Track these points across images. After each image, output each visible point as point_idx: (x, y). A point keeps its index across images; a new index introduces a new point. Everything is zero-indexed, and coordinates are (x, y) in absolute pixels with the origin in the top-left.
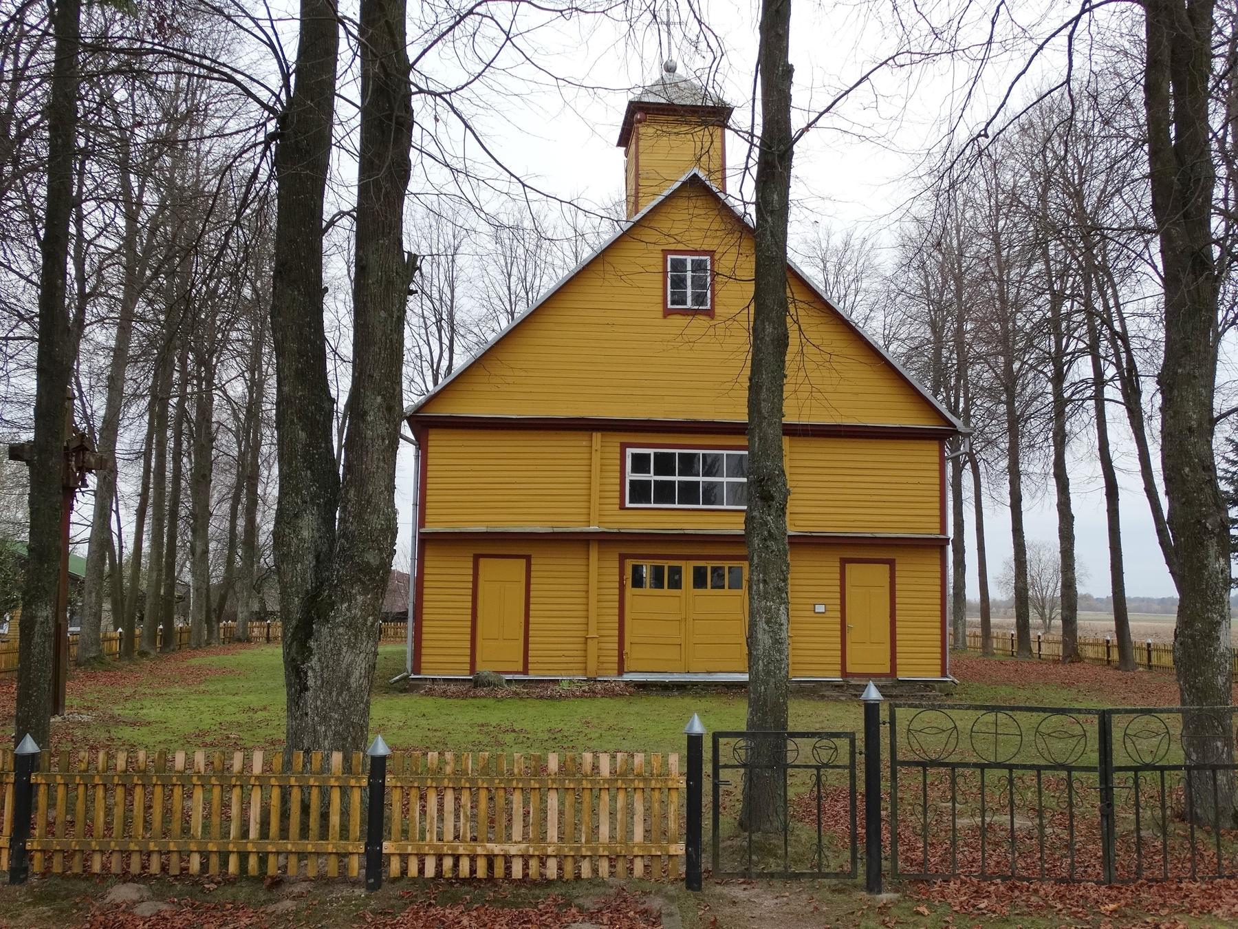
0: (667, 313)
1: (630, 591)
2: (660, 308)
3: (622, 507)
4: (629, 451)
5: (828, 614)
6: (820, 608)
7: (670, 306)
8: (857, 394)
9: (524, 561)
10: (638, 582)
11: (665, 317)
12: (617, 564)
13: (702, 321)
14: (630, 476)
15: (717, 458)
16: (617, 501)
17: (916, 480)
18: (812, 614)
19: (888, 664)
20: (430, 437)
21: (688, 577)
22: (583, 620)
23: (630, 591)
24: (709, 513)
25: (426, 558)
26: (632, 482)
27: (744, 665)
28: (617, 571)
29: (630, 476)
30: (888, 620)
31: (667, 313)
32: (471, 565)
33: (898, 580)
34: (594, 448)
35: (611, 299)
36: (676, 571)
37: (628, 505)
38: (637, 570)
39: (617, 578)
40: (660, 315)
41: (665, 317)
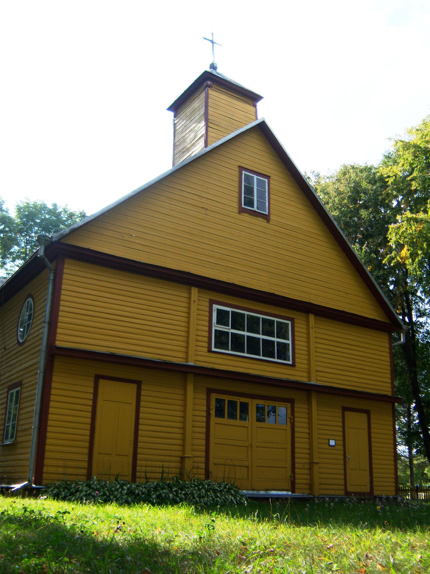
0: (241, 211)
1: (214, 419)
2: (236, 205)
3: (210, 351)
4: (215, 307)
5: (337, 447)
6: (332, 443)
7: (243, 206)
8: (347, 293)
9: (134, 387)
10: (220, 413)
11: (239, 213)
12: (205, 397)
13: (260, 221)
14: (216, 327)
15: (271, 323)
16: (206, 345)
17: (379, 357)
18: (327, 446)
19: (369, 486)
20: (66, 266)
21: (427, 118)
22: (180, 442)
23: (214, 419)
24: (266, 364)
25: (54, 379)
26: (216, 331)
27: (288, 485)
28: (204, 402)
29: (216, 327)
30: (368, 453)
31: (241, 211)
32: (92, 384)
33: (372, 426)
34: (193, 299)
35: (206, 191)
36: (244, 407)
37: (213, 349)
38: (219, 402)
39: (205, 408)
40: (236, 211)
41: (239, 213)
